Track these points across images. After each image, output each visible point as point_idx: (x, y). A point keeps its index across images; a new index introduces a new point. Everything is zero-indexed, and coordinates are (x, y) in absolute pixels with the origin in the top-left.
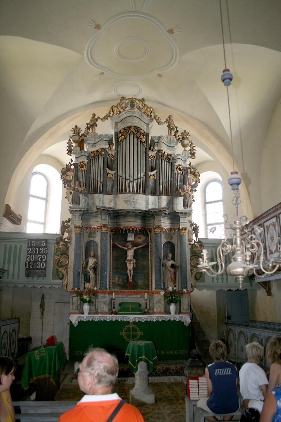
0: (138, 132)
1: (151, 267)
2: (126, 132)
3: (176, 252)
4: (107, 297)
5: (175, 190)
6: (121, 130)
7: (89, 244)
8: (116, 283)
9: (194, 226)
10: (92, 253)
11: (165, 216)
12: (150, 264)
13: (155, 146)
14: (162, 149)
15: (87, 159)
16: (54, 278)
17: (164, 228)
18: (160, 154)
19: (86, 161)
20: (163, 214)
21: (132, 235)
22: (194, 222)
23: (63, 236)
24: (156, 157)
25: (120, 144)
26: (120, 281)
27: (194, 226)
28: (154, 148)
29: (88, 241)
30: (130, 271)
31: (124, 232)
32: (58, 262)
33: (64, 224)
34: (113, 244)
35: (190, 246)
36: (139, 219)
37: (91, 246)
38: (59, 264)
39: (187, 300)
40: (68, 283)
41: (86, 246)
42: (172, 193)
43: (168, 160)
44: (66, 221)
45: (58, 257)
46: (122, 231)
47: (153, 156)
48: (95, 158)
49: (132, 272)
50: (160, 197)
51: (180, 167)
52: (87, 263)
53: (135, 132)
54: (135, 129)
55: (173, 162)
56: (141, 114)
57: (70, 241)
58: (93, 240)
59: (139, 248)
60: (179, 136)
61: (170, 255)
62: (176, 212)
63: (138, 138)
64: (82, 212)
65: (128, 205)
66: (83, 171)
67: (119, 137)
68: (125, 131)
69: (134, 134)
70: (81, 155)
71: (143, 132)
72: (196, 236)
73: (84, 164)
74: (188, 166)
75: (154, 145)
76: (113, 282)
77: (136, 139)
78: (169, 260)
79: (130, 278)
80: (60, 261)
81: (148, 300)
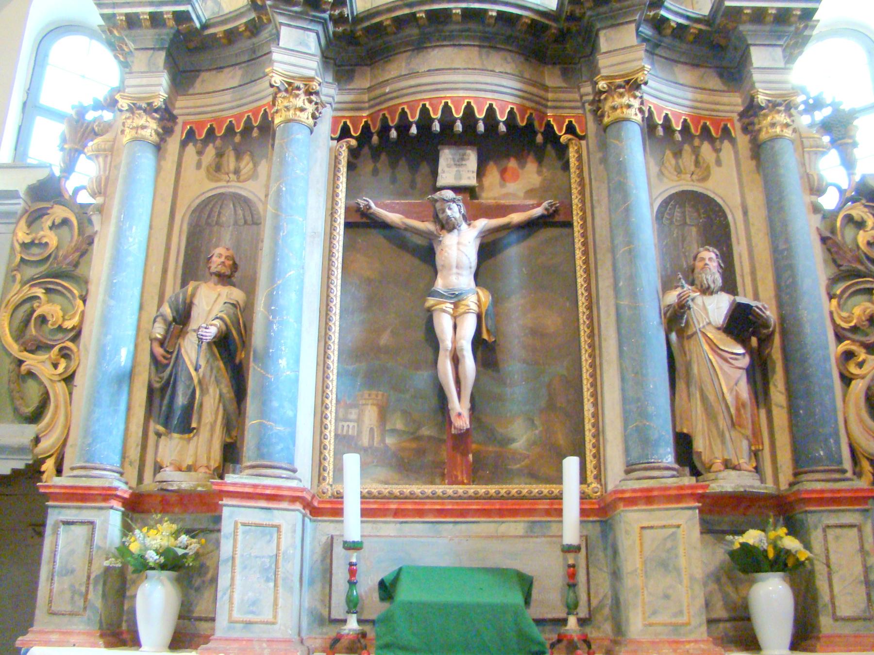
1: (591, 336)
3: (740, 250)
4: (283, 529)
7: (211, 210)
10: (218, 257)
11: (657, 46)
12: (582, 318)
17: (660, 109)
20: (647, 31)
23: (67, 178)
26: (394, 431)
29: (203, 198)
30: (456, 360)
32: (26, 322)
35: (816, 221)
36: (505, 59)
37: (217, 223)
38: (32, 330)
40: (70, 442)
41: (190, 224)
45: (28, 291)
58: (232, 190)
61: (710, 257)
64: (166, 31)
78: (706, 291)
80: (35, 315)
81: (583, 550)
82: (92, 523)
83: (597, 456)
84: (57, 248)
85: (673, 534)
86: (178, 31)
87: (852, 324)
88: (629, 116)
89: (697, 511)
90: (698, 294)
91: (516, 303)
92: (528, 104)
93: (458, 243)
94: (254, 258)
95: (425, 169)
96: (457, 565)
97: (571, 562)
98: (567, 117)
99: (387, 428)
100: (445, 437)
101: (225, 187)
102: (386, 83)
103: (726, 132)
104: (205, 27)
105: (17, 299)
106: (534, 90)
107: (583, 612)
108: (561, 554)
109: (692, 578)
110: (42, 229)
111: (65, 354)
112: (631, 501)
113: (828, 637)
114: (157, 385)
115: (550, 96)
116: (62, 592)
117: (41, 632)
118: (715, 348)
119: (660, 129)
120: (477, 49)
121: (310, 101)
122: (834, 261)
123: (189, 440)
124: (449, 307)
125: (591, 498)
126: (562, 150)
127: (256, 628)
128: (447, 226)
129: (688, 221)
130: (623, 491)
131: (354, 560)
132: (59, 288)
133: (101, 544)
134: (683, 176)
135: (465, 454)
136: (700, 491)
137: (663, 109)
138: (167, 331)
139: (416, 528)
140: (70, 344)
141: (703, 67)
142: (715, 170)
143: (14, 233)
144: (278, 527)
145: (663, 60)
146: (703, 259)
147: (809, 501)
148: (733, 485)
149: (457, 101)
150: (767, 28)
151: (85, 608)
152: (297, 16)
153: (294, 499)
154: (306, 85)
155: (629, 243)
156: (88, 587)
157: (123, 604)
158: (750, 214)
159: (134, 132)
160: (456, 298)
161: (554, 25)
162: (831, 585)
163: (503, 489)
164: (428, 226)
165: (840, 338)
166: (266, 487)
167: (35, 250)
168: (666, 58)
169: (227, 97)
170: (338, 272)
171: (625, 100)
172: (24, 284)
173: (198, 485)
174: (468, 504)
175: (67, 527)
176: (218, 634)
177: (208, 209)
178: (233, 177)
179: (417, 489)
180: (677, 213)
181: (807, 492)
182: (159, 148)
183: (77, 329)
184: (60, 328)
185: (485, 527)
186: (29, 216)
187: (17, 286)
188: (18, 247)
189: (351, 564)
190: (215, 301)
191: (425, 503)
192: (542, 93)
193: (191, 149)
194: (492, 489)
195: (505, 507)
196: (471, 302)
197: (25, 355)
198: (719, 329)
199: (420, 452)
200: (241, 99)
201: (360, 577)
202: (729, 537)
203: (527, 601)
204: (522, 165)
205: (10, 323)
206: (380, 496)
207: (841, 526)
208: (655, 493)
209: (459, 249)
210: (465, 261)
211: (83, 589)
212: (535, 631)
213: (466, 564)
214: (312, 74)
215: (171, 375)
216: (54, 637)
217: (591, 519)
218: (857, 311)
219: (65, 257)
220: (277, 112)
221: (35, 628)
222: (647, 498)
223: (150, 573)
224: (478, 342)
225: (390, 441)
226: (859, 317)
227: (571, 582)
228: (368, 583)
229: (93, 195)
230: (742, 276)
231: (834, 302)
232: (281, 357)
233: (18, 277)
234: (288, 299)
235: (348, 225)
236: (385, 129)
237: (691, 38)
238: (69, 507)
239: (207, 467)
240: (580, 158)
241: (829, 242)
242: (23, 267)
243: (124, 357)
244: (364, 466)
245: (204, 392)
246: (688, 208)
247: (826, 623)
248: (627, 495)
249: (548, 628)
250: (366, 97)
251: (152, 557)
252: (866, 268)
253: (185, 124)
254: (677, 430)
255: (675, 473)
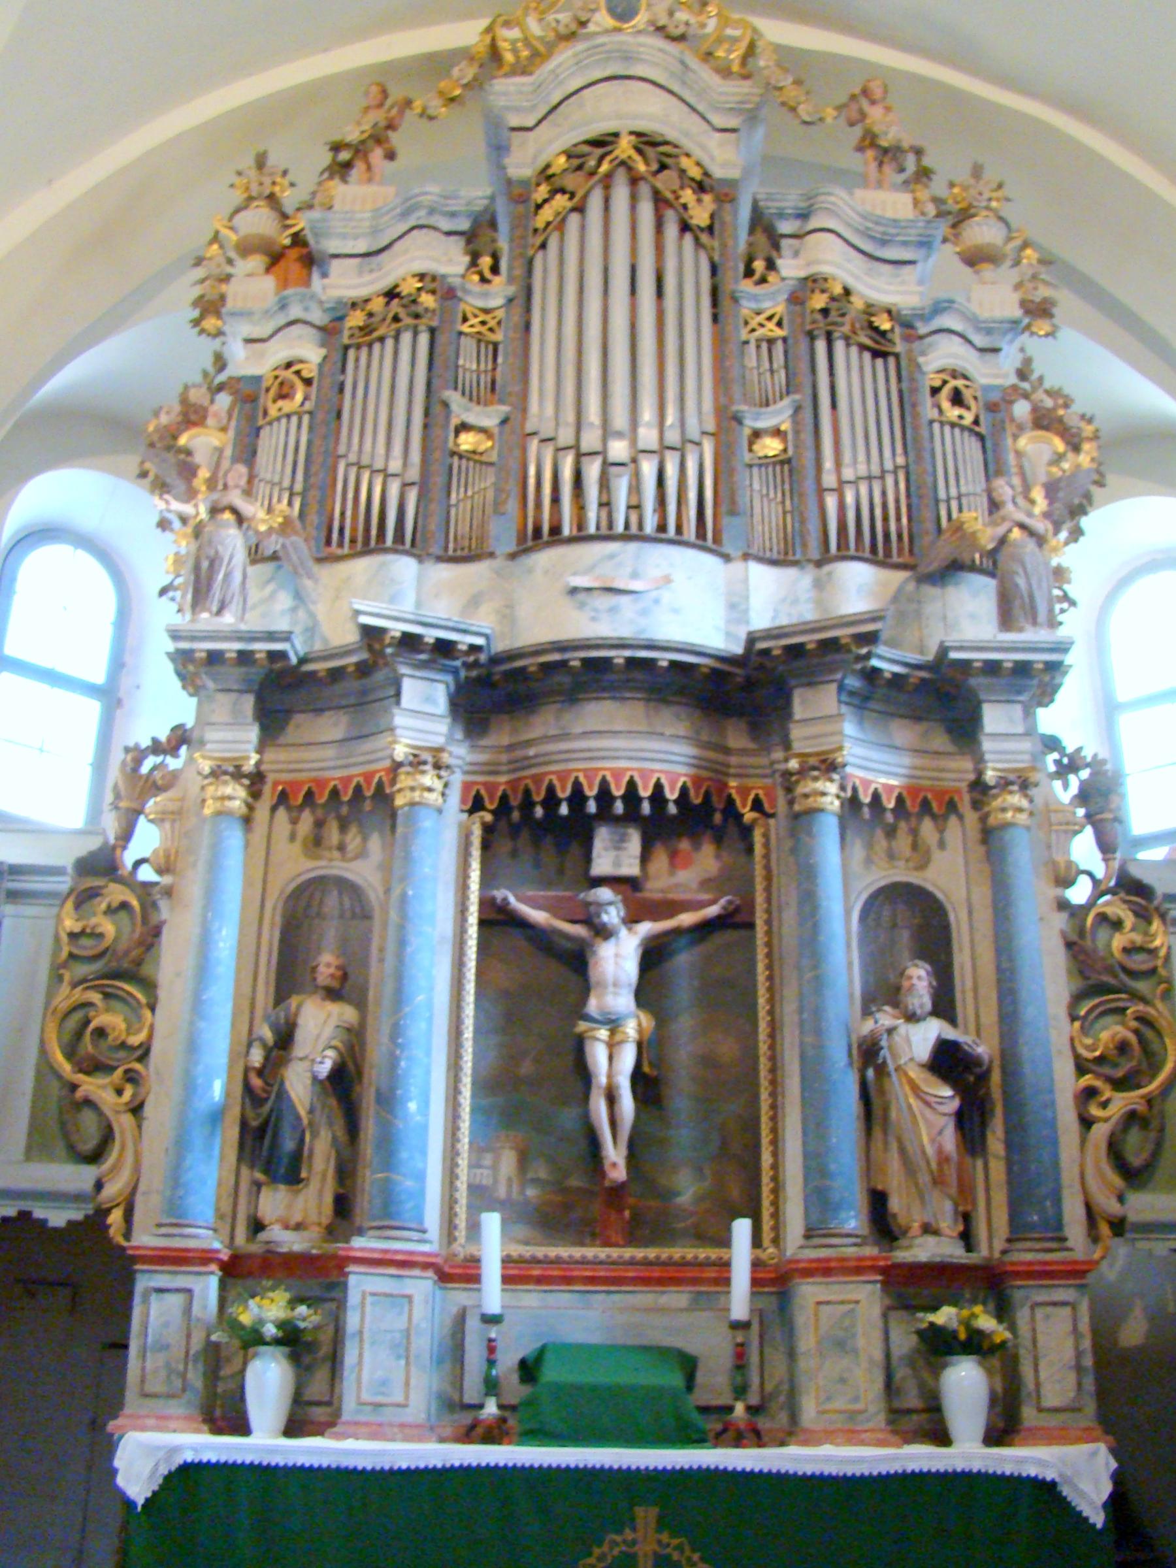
0: (663, 167)
1: (773, 1070)
2: (580, 168)
3: (961, 959)
4: (417, 1299)
5: (930, 526)
6: (548, 166)
7: (312, 896)
8: (502, 1192)
9: (1085, 774)
10: (327, 964)
11: (867, 699)
12: (763, 1048)
13: (780, 257)
14: (826, 269)
15: (323, 345)
16: (36, 1148)
17: (866, 783)
18: (819, 301)
19: (311, 353)
20: (853, 682)
21: (623, 839)
22: (1079, 750)
23: (124, 848)
24: (792, 322)
25: (543, 246)
27: (1085, 774)
28: (771, 265)
31: (564, 810)
32: (79, 1035)
33: (138, 762)
34: (487, 904)
36: (678, 716)
37: (319, 915)
38: (87, 1045)
39: (1069, 1327)
40: (142, 1187)
41: (284, 916)
42: (911, 551)
43: (877, 342)
44: (157, 748)
45: (79, 995)
46: (551, 800)
47: (770, 318)
48: (375, 335)
49: (627, 1103)
50: (827, 569)
51: (960, 383)
52: (285, 1039)
53: (641, 167)
54: (639, 151)
55: (910, 351)
56: (682, 63)
57: (166, 880)
59: (677, 932)
60: (937, 201)
61: (919, 978)
62: (954, 655)
63: (659, 201)
64: (253, 670)
65: (594, 619)
66: (288, 416)
67: (539, 207)
68: (576, 162)
69: (634, 181)
70: (282, 320)
71: (695, 173)
72: (1106, 847)
73: (298, 373)
74: (1013, 379)
75: (774, 254)
76: (473, 1188)
77: (646, 210)
78: (912, 1018)
79: (615, 1155)
80: (92, 1026)
81: (755, 1327)
82: (189, 1291)
83: (776, 1215)
84: (116, 939)
85: (852, 1311)
86: (271, 671)
87: (1097, 1053)
88: (822, 806)
89: (879, 1286)
90: (901, 1021)
91: (685, 1024)
92: (705, 774)
93: (617, 955)
94: (365, 964)
95: (575, 849)
96: (609, 1342)
97: (739, 1339)
98: (753, 788)
99: (530, 1175)
100: (597, 1189)
101: (326, 867)
102: (529, 743)
103: (952, 807)
104: (303, 661)
105: (64, 1006)
106: (712, 755)
107: (754, 1399)
108: (730, 1331)
109: (871, 1361)
110: (95, 914)
111: (132, 1077)
112: (808, 1273)
113: (1030, 1429)
114: (254, 1123)
115: (734, 760)
116: (156, 1370)
117: (131, 1416)
118: (915, 1089)
119: (866, 810)
120: (642, 703)
121: (439, 777)
122: (1081, 972)
123: (299, 1191)
124: (603, 1033)
125: (766, 1266)
126: (746, 832)
127: (388, 1411)
128: (604, 933)
129: (900, 923)
130: (798, 1261)
131: (493, 1335)
132: (120, 993)
133: (200, 1315)
134: (897, 863)
135: (621, 1211)
136: (882, 1263)
137: (870, 782)
138: (267, 1058)
139: (562, 1299)
140: (137, 1066)
141: (927, 719)
142: (937, 855)
143: (59, 919)
144: (409, 1298)
145: (875, 715)
146: (910, 978)
147: (1017, 1274)
148: (929, 1254)
149: (618, 774)
150: (1003, 681)
151: (184, 1390)
152: (423, 665)
153: (426, 1266)
154: (434, 757)
155: (816, 967)
156: (186, 1364)
157: (215, 1386)
158: (975, 914)
159: (218, 804)
160: (613, 1024)
161: (738, 671)
162: (1036, 1370)
163: (665, 1253)
164: (579, 930)
165: (1081, 1068)
166: (397, 1252)
167: (85, 941)
168: (880, 712)
169: (330, 752)
170: (470, 987)
171: (820, 785)
172: (74, 985)
173: (313, 1247)
174: (626, 1271)
175: (161, 1295)
176: (346, 1416)
177: (307, 894)
178: (336, 854)
179: (565, 1252)
180: (886, 913)
181: (1013, 1264)
182: (247, 821)
183: (145, 1046)
184: (123, 1045)
185: (644, 1297)
186: (77, 898)
187: (65, 989)
188: (64, 938)
189: (490, 1340)
190: (325, 1022)
191: (572, 1270)
192: (720, 757)
193: (282, 813)
194: (651, 1253)
195: (665, 1275)
196: (630, 1029)
197: (81, 1077)
198: (923, 1066)
199: (567, 1207)
200: (347, 757)
201: (499, 1355)
202: (920, 1315)
203: (690, 1383)
204: (697, 846)
205: (59, 1040)
206: (521, 1260)
207: (1054, 1304)
208: (833, 1264)
209: (616, 964)
210: (624, 978)
211: (181, 1367)
212: (696, 1417)
213: (620, 1341)
214: (439, 741)
215: (272, 1111)
216: (151, 1422)
217: (766, 1289)
218: (1105, 1036)
219: (127, 953)
220: (400, 790)
221: (127, 1410)
222: (824, 1269)
223: (262, 1349)
224: (638, 1076)
225: (531, 1192)
226: (1106, 1046)
227: (739, 1363)
228: (508, 1361)
229: (160, 872)
230: (963, 992)
231: (1077, 1024)
232: (410, 1099)
233: (67, 976)
234: (416, 1029)
235: (482, 923)
236: (528, 804)
237: (910, 688)
238: (162, 1272)
239: (319, 1224)
240: (767, 845)
241: (1076, 948)
242: (71, 963)
243: (217, 1089)
244: (504, 1222)
245: (315, 1135)
246: (901, 907)
247: (1028, 1414)
248: (802, 1265)
249: (713, 1417)
250: (504, 758)
251: (270, 1330)
252: (1121, 981)
253: (276, 784)
254: (872, 1184)
255: (859, 1240)
